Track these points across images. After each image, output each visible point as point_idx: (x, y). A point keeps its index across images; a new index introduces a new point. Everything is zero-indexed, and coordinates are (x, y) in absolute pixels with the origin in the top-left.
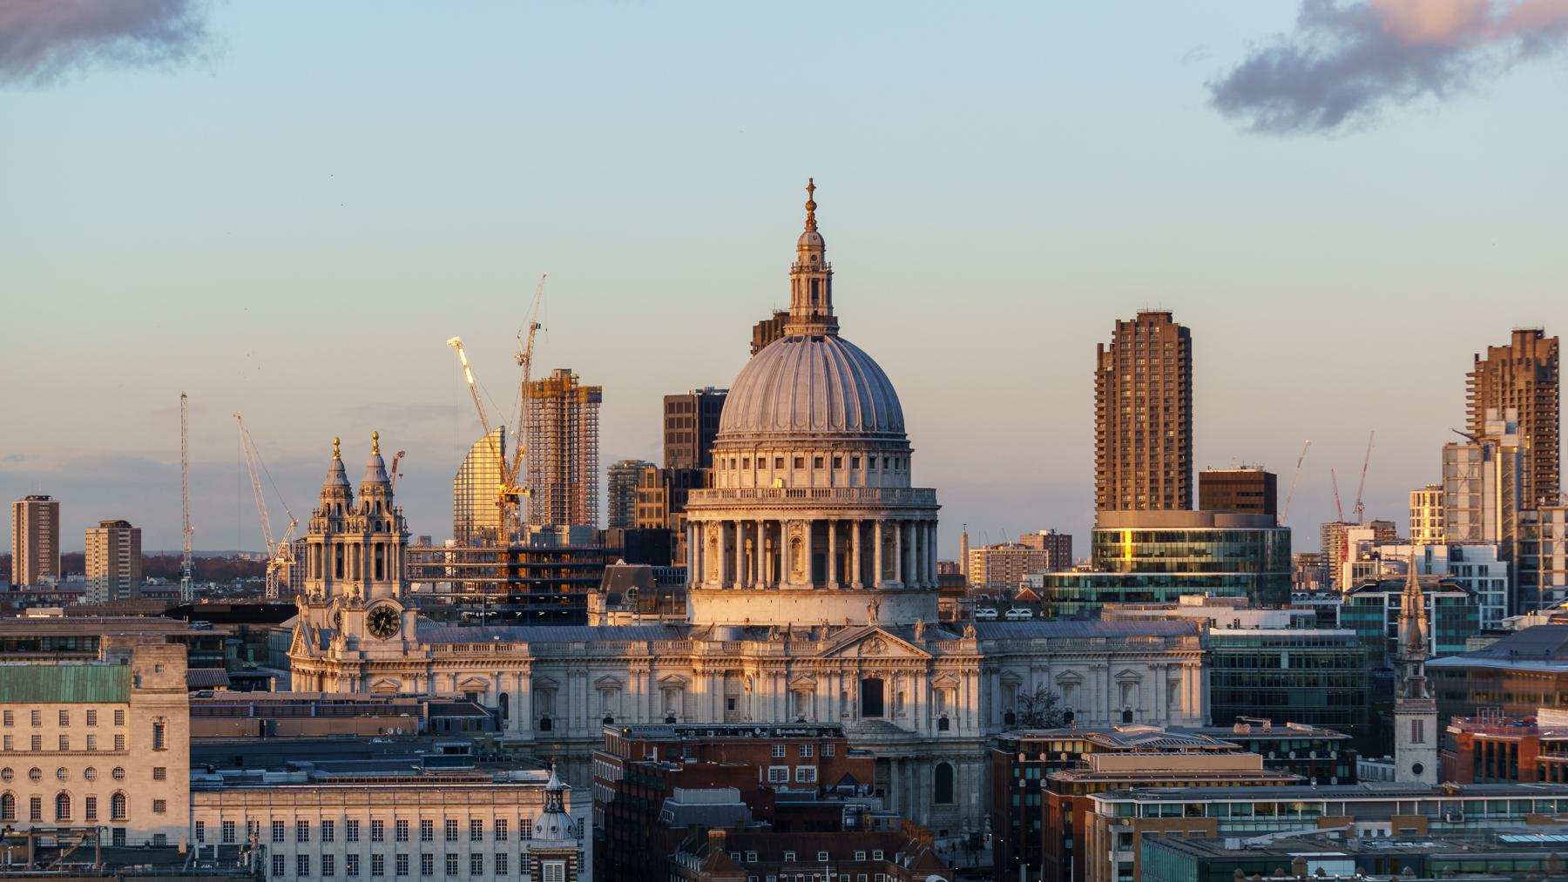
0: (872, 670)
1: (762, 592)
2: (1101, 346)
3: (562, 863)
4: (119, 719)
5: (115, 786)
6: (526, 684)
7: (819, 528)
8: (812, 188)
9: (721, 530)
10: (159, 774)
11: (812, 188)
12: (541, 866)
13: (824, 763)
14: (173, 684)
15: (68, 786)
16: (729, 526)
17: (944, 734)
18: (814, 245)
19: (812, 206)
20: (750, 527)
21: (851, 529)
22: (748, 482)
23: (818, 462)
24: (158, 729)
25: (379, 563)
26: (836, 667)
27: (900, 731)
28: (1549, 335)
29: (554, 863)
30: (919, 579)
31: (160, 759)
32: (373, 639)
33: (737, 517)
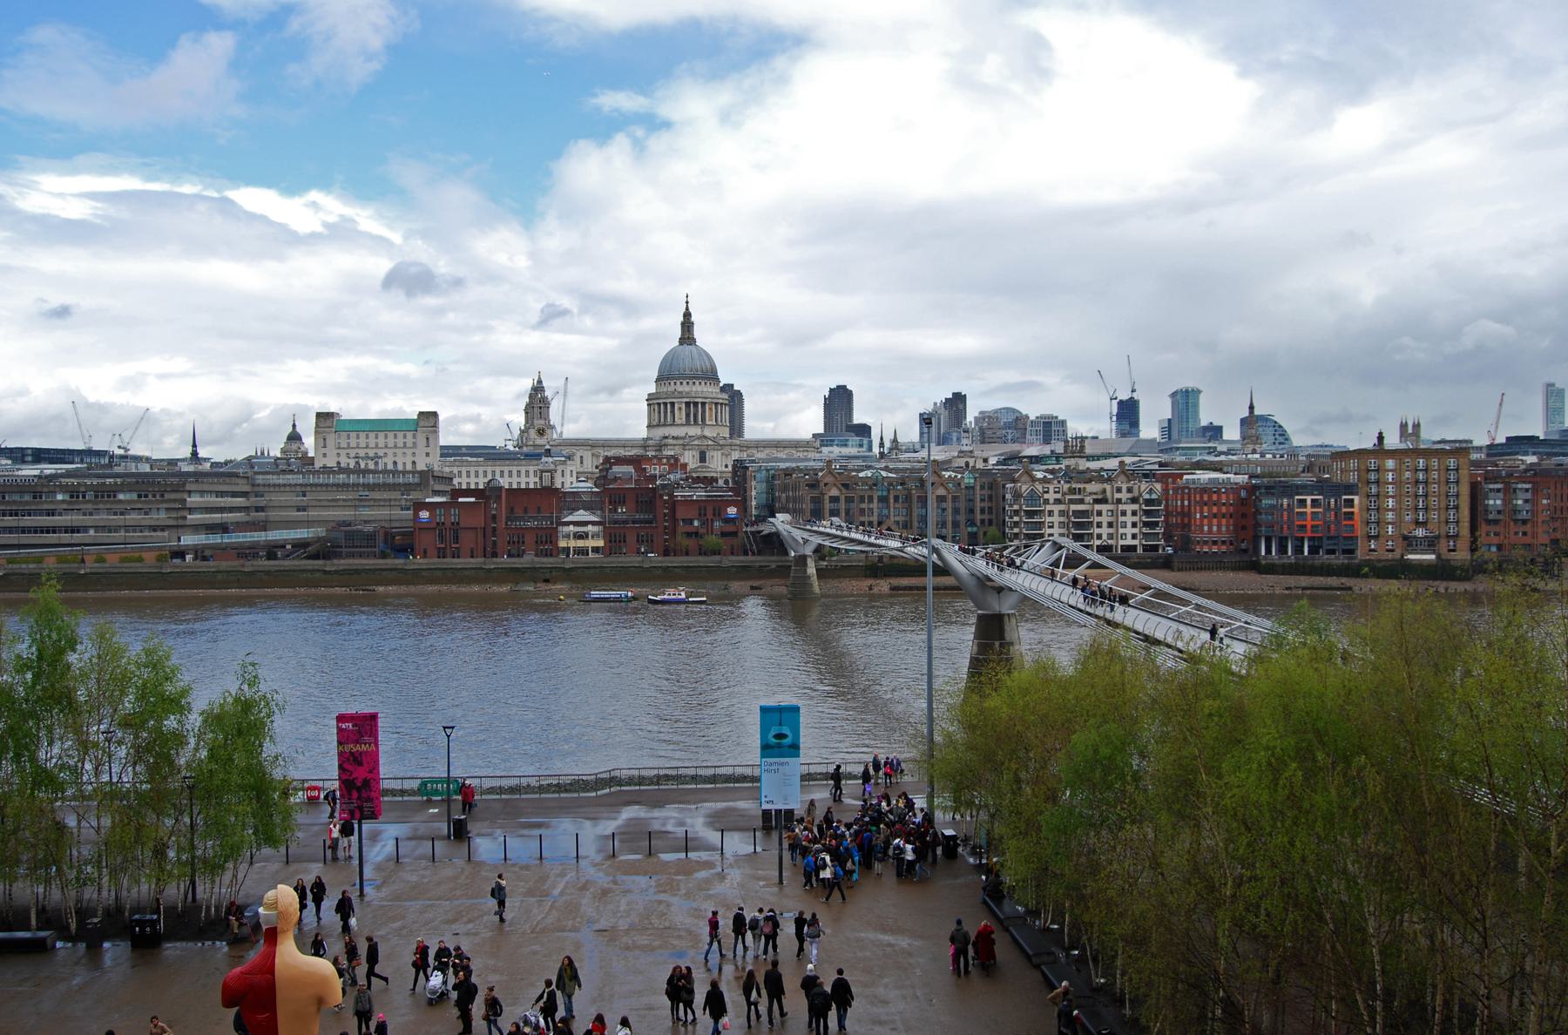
0: (703, 448)
1: (670, 425)
4: (414, 437)
5: (413, 459)
6: (590, 453)
7: (688, 404)
10: (427, 455)
13: (671, 466)
15: (396, 459)
16: (659, 404)
18: (687, 315)
19: (687, 302)
31: (428, 450)
33: (661, 401)
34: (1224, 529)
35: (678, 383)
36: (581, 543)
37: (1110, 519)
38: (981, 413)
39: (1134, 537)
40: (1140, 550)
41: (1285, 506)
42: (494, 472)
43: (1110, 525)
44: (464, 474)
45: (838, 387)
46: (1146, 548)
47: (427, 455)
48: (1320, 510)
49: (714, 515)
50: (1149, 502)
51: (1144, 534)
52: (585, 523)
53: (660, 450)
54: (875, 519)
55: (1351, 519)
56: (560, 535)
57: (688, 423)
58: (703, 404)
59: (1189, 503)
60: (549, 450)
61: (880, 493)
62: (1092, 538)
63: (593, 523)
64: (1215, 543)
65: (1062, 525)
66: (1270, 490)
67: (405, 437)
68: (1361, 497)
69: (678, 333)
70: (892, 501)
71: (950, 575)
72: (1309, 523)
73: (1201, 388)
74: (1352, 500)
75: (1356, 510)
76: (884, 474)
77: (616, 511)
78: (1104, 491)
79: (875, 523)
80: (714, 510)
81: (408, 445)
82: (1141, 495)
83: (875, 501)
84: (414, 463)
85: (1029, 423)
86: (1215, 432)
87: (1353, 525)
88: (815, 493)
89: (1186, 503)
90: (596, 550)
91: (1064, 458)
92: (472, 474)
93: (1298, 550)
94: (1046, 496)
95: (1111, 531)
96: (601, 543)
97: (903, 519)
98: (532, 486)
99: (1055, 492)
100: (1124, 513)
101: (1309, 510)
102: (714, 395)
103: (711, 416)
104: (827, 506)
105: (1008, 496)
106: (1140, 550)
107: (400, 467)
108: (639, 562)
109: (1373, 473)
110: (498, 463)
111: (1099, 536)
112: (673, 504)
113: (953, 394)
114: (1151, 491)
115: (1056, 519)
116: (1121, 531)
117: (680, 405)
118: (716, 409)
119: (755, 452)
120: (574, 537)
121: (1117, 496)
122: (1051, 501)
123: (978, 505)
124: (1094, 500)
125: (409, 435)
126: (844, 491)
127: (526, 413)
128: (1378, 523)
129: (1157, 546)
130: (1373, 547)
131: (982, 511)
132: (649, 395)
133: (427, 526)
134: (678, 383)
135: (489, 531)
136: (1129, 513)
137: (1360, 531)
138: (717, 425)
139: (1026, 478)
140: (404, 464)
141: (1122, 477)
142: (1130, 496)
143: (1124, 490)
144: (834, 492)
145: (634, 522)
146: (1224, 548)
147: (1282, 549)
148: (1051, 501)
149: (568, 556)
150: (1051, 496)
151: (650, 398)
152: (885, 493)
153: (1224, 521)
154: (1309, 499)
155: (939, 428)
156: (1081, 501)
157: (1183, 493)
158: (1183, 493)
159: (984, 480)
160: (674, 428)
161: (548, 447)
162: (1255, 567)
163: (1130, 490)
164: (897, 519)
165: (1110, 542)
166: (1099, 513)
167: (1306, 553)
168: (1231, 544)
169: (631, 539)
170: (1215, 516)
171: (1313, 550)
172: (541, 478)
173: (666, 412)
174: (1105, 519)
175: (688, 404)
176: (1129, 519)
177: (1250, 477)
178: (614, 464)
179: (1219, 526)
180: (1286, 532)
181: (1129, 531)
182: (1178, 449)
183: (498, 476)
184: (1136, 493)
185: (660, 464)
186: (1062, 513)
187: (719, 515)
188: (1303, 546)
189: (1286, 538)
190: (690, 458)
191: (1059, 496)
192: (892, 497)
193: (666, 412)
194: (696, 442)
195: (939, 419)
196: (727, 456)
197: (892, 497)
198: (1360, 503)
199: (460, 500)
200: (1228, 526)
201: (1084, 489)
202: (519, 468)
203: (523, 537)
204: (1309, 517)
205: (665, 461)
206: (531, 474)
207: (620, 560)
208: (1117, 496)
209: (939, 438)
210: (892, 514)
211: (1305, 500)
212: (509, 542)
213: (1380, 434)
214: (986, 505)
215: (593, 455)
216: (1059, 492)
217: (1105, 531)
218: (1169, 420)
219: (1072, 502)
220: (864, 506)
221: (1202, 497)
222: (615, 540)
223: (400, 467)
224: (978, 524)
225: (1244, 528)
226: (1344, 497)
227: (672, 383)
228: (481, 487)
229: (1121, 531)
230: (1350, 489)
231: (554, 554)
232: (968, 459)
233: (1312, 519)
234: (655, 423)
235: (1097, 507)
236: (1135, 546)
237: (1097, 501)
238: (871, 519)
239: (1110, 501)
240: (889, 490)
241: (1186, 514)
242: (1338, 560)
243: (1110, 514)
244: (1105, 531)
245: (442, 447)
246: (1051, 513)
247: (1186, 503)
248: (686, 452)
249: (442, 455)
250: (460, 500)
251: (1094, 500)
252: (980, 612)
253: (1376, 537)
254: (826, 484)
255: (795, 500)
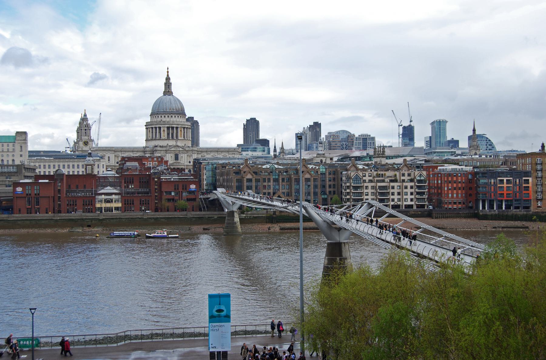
0: (177, 152)
2: (244, 124)
3: (91, 167)
4: (14, 146)
5: (13, 158)
6: (113, 155)
7: (168, 128)
8: (168, 69)
9: (151, 129)
11: (168, 69)
12: (86, 167)
13: (159, 162)
14: (24, 139)
15: (3, 158)
16: (152, 128)
17: (190, 164)
18: (168, 79)
19: (168, 72)
20: (156, 128)
21: (174, 128)
22: (156, 120)
23: (168, 116)
24: (21, 147)
25: (86, 133)
26: (170, 152)
27: (180, 163)
28: (319, 123)
29: (89, 167)
30: (187, 138)
31: (21, 153)
32: (84, 146)
33: (153, 126)
34: (460, 195)
35: (163, 116)
36: (108, 205)
37: (399, 191)
38: (329, 133)
39: (412, 200)
40: (415, 207)
41: (492, 183)
42: (59, 165)
43: (399, 194)
44: (42, 166)
45: (251, 119)
46: (418, 206)
47: (21, 156)
48: (511, 185)
49: (183, 189)
50: (419, 181)
51: (417, 198)
52: (111, 194)
53: (153, 153)
54: (271, 191)
55: (528, 190)
56: (97, 200)
57: (168, 139)
58: (177, 128)
59: (441, 182)
60: (91, 153)
61: (274, 177)
62: (389, 201)
63: (115, 194)
64: (455, 203)
65: (373, 194)
66: (484, 175)
67: (8, 146)
68: (533, 178)
69: (163, 89)
70: (281, 181)
71: (312, 221)
72: (505, 192)
73: (447, 120)
74: (528, 180)
75: (530, 185)
76: (276, 166)
77: (128, 187)
78: (395, 175)
79: (272, 193)
80: (183, 186)
81: (10, 150)
82: (415, 177)
83: (272, 181)
84: (13, 160)
85: (355, 138)
86: (455, 143)
87: (529, 194)
88: (239, 177)
89: (439, 182)
90: (117, 209)
91: (374, 157)
92: (47, 167)
93: (500, 207)
94: (364, 178)
95: (399, 197)
96: (120, 205)
97: (287, 191)
98: (81, 173)
99: (369, 176)
100: (406, 187)
101: (505, 185)
102: (181, 123)
103: (181, 135)
104: (245, 184)
105: (344, 178)
106: (415, 207)
107: (5, 163)
108: (141, 215)
109: (539, 166)
110: (62, 160)
111: (393, 200)
112: (160, 183)
113: (314, 122)
114: (421, 175)
115: (370, 191)
116: (405, 197)
117: (164, 129)
118: (184, 133)
119: (205, 154)
120: (105, 202)
121: (402, 178)
122: (367, 181)
123: (328, 183)
124: (390, 180)
125: (11, 145)
126: (255, 176)
127: (78, 133)
128: (542, 192)
129: (424, 205)
130: (539, 205)
131: (330, 186)
132: (147, 123)
133: (21, 196)
134: (163, 116)
135: (56, 198)
136: (409, 187)
137: (533, 196)
138: (184, 139)
139: (353, 168)
140: (8, 161)
141: (405, 168)
142: (409, 178)
143: (406, 175)
144: (249, 176)
145: (138, 193)
146: (460, 206)
147: (491, 207)
148: (367, 181)
149: (101, 212)
150: (367, 178)
151: (147, 125)
152: (277, 177)
153: (460, 191)
154: (505, 179)
155: (306, 142)
156: (383, 181)
157: (438, 176)
158: (438, 176)
159: (331, 170)
160: (160, 141)
161: (90, 152)
162: (477, 216)
163: (409, 175)
164: (284, 191)
165: (399, 203)
166: (393, 188)
167: (504, 209)
168: (464, 204)
169: (137, 202)
170: (455, 189)
171: (508, 207)
172: (86, 169)
173: (156, 133)
174: (396, 191)
175: (168, 128)
176: (409, 191)
177: (474, 168)
178: (127, 161)
179: (457, 194)
180: (493, 198)
181: (409, 197)
182: (435, 152)
183: (61, 168)
184: (412, 177)
185: (153, 161)
186: (373, 187)
187: (186, 189)
188: (502, 205)
189: (493, 201)
190: (169, 158)
191: (371, 178)
192: (280, 179)
193: (156, 133)
194: (173, 149)
195: (306, 136)
196: (190, 156)
197: (280, 179)
198: (533, 181)
199: (40, 181)
200: (462, 195)
201: (385, 174)
202: (73, 163)
203: (76, 202)
204: (505, 189)
205: (155, 159)
206: (81, 166)
207: (130, 214)
208: (402, 178)
209: (306, 147)
210: (281, 188)
211: (503, 180)
212: (68, 205)
213: (543, 144)
214: (332, 183)
215: (115, 156)
216: (371, 176)
217: (396, 197)
218: (430, 137)
219: (378, 181)
220: (265, 184)
221: (448, 179)
222: (128, 204)
223: (5, 163)
224: (328, 194)
225: (470, 195)
226: (524, 178)
227: (160, 116)
228: (52, 174)
229: (405, 197)
230: (527, 174)
231: (93, 211)
232: (322, 158)
233: (507, 191)
234: (150, 139)
235: (392, 184)
236: (412, 205)
237: (392, 181)
238: (269, 191)
239: (399, 181)
240: (279, 175)
241: (439, 187)
242: (521, 212)
243: (398, 188)
244: (396, 197)
245: (30, 152)
246: (367, 187)
247: (439, 182)
248: (168, 155)
249: (30, 156)
250: (40, 181)
251: (390, 180)
252: (329, 241)
253: (541, 200)
254: (244, 172)
255: (228, 181)
